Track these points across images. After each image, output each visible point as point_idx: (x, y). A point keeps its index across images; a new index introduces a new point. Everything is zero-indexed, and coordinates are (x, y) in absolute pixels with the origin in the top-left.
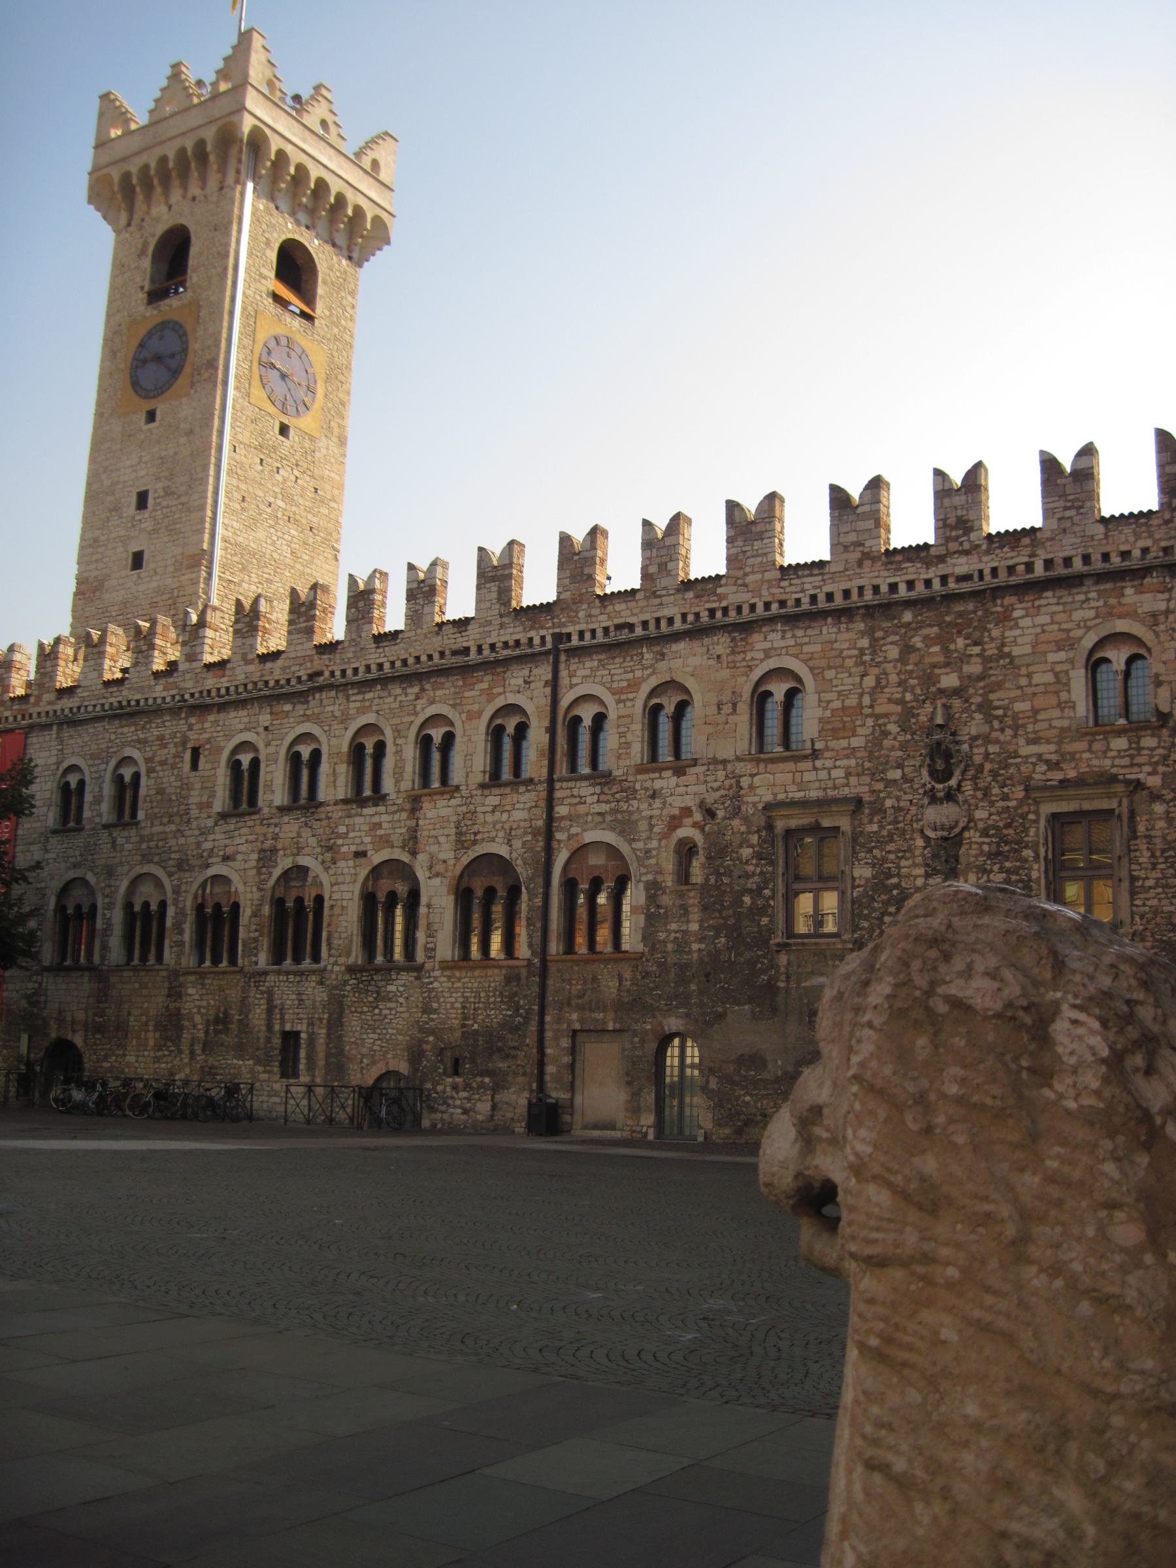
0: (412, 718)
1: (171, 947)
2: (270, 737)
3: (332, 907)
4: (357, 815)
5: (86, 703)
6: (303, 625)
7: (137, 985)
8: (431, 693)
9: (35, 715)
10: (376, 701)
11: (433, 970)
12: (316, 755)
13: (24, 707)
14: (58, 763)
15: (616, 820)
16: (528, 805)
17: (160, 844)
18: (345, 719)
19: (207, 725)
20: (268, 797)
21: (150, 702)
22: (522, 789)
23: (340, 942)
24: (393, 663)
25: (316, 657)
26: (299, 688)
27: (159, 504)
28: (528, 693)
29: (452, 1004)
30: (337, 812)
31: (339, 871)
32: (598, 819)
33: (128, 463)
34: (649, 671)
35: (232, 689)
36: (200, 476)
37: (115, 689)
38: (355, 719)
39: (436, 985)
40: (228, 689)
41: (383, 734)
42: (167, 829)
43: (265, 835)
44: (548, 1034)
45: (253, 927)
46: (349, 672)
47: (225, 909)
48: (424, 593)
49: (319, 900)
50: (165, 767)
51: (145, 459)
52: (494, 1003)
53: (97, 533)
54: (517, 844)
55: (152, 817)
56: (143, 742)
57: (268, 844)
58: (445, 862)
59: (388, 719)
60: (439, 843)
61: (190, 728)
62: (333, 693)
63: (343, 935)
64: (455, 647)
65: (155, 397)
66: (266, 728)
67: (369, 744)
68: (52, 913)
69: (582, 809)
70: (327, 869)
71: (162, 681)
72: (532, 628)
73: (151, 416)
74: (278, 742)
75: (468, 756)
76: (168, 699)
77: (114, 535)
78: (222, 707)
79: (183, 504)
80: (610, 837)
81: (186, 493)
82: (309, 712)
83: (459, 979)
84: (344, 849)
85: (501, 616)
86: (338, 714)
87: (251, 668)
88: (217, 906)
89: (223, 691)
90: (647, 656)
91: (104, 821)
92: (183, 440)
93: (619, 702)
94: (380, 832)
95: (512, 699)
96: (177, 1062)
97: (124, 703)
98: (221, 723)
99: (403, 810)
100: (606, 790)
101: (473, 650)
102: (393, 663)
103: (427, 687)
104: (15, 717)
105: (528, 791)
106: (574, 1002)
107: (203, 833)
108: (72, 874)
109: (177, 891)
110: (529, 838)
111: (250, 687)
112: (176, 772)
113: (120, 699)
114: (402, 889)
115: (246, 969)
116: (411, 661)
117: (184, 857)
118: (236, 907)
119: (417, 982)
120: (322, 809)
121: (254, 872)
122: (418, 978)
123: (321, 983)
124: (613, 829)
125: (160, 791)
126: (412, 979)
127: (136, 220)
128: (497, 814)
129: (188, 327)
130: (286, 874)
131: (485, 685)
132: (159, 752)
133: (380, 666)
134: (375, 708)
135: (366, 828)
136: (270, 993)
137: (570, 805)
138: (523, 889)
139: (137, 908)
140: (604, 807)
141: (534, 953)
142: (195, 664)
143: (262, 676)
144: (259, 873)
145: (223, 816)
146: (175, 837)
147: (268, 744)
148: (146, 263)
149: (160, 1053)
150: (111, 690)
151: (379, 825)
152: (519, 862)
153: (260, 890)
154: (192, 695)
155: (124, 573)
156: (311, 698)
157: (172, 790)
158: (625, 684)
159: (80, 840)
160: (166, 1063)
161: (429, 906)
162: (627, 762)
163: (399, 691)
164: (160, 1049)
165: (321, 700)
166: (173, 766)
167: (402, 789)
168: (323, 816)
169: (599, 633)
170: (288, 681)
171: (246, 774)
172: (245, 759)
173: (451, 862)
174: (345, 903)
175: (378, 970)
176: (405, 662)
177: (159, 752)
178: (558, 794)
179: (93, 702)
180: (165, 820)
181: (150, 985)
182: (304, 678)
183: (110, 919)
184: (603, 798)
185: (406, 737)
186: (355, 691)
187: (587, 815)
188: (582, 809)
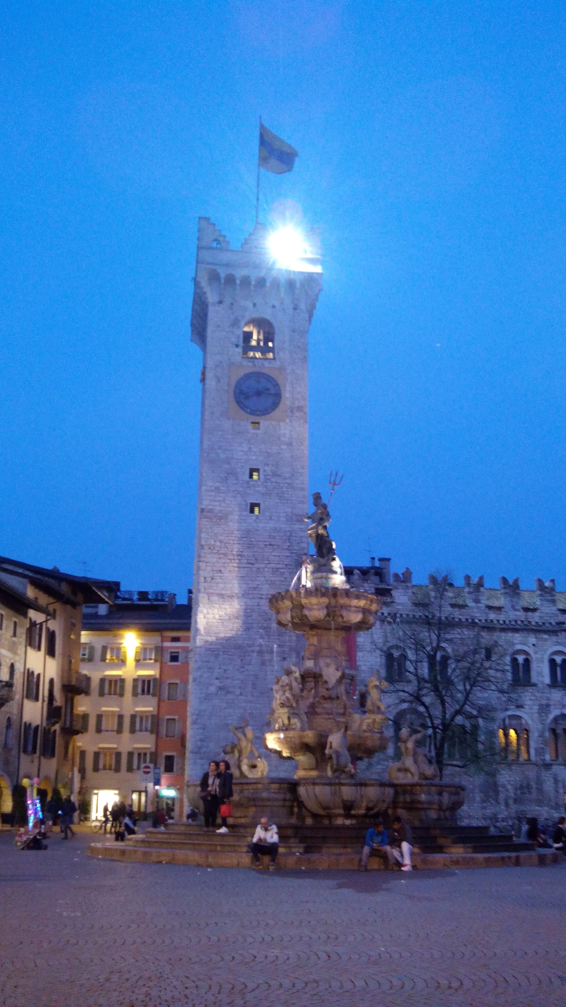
26: (550, 628)
35: (507, 622)
40: (504, 621)
53: (218, 484)
57: (544, 702)
65: (258, 415)
79: (289, 484)
81: (290, 478)
87: (518, 613)
89: (501, 622)
92: (284, 447)
96: (498, 809)
127: (227, 301)
129: (280, 382)
142: (479, 605)
143: (527, 618)
144: (540, 716)
147: (536, 653)
149: (484, 805)
155: (245, 513)
156: (559, 634)
160: (491, 810)
164: (484, 801)
172: (521, 659)
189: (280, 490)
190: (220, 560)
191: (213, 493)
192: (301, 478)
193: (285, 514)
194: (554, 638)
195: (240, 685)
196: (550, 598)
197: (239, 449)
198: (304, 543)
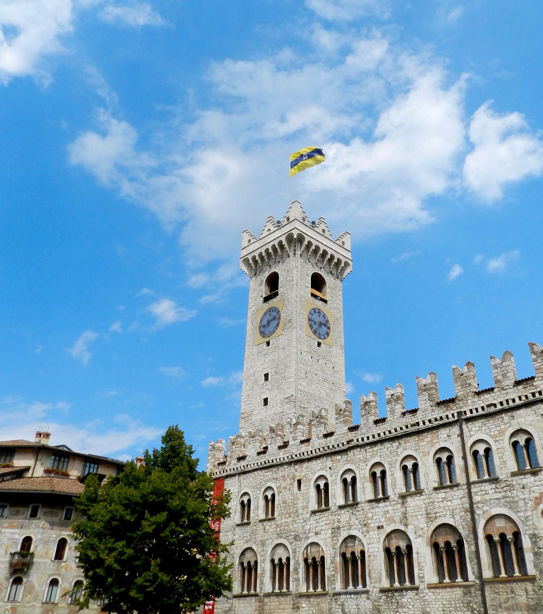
0: (397, 458)
1: (293, 582)
2: (332, 472)
3: (369, 556)
4: (376, 507)
5: (250, 463)
6: (343, 419)
7: (278, 603)
9: (228, 470)
10: (379, 451)
14: (239, 492)
16: (460, 497)
17: (286, 528)
18: (366, 461)
19: (303, 469)
20: (334, 501)
21: (278, 460)
22: (455, 489)
23: (375, 575)
24: (384, 433)
27: (273, 378)
28: (450, 441)
29: (437, 608)
30: (367, 506)
31: (371, 537)
33: (260, 363)
37: (263, 455)
38: (370, 460)
39: (427, 597)
40: (311, 451)
42: (288, 520)
43: (334, 520)
45: (332, 569)
46: (365, 439)
47: (317, 560)
48: (394, 400)
49: (363, 553)
50: (286, 490)
52: (460, 607)
54: (457, 517)
55: (281, 515)
56: (276, 479)
58: (422, 529)
59: (385, 459)
60: (418, 519)
61: (296, 471)
62: (359, 449)
63: (376, 571)
64: (413, 423)
66: (330, 468)
67: (378, 471)
68: (237, 566)
69: (487, 497)
70: (365, 536)
71: (283, 450)
74: (336, 474)
76: (286, 458)
78: (309, 460)
82: (349, 459)
84: (372, 525)
85: (432, 406)
86: (362, 459)
88: (314, 559)
89: (309, 453)
91: (260, 519)
94: (388, 516)
95: (443, 445)
97: (267, 462)
98: (310, 467)
99: (398, 503)
101: (421, 424)
102: (384, 433)
103: (402, 442)
105: (458, 490)
107: (305, 521)
108: (246, 546)
109: (294, 552)
110: (463, 514)
111: (321, 449)
112: (291, 492)
113: (265, 460)
114: (403, 545)
115: (330, 592)
116: (393, 431)
117: (297, 534)
118: (323, 558)
119: (416, 597)
120: (359, 506)
121: (330, 539)
122: (417, 594)
123: (368, 598)
125: (284, 502)
126: (415, 594)
130: (345, 540)
131: (429, 439)
132: (283, 483)
134: (378, 455)
135: (381, 514)
136: (343, 605)
137: (481, 495)
138: (465, 542)
139: (276, 562)
142: (296, 441)
143: (326, 444)
145: (314, 512)
146: (292, 524)
150: (261, 456)
151: (388, 512)
153: (333, 548)
155: (260, 408)
157: (290, 501)
159: (249, 528)
161: (417, 553)
165: (354, 453)
166: (290, 490)
167: (396, 493)
168: (360, 509)
170: (338, 445)
171: (323, 491)
172: (322, 483)
173: (425, 529)
174: (375, 554)
175: (396, 590)
176: (390, 432)
177: (283, 483)
179: (253, 462)
180: (287, 516)
181: (284, 602)
182: (345, 443)
183: (264, 568)
185: (395, 467)
186: (369, 447)
187: (490, 500)
188: (487, 497)
191: (246, 400)
194: (345, 457)
196: (343, 419)
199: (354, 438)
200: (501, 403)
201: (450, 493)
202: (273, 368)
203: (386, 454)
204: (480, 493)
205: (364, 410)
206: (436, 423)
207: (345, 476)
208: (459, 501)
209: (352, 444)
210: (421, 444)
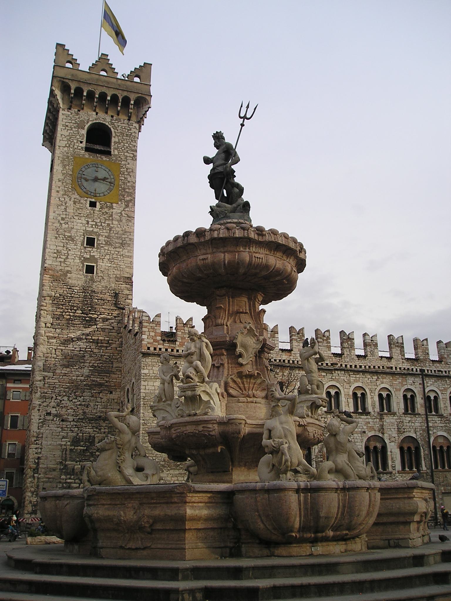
0: (376, 387)
4: (359, 418)
8: (382, 380)
10: (361, 378)
11: (396, 474)
12: (337, 394)
13: (172, 345)
15: (446, 429)
18: (349, 383)
22: (417, 416)
25: (333, 357)
26: (327, 368)
31: (355, 438)
32: (441, 428)
34: (449, 386)
36: (128, 243)
39: (397, 479)
40: (293, 361)
41: (364, 390)
44: (436, 494)
46: (348, 366)
48: (374, 345)
51: (90, 223)
53: (59, 248)
54: (418, 434)
58: (394, 437)
62: (343, 372)
64: (388, 366)
72: (413, 365)
73: (93, 205)
75: (398, 403)
77: (73, 253)
79: (118, 252)
80: (445, 434)
82: (333, 377)
83: (405, 477)
89: (291, 362)
90: (448, 381)
93: (442, 394)
99: (377, 418)
100: (442, 419)
101: (394, 369)
102: (365, 366)
104: (166, 350)
106: (441, 484)
110: (422, 432)
114: (379, 445)
116: (372, 367)
119: (390, 478)
122: (390, 477)
124: (445, 432)
128: (410, 423)
131: (400, 381)
133: (361, 367)
134: (361, 381)
140: (442, 425)
141: (427, 469)
148: (84, 132)
152: (419, 439)
154: (275, 360)
156: (333, 372)
158: (443, 389)
161: (391, 452)
162: (447, 412)
163: (369, 377)
167: (375, 411)
169: (433, 372)
173: (397, 438)
178: (429, 419)
182: (329, 364)
184: (442, 422)
186: (352, 373)
189: (111, 256)
190: (58, 310)
191: (56, 255)
192: (129, 248)
193: (115, 276)
194: (329, 376)
195: (73, 413)
197: (80, 221)
198: (129, 299)
199: (338, 363)
200: (446, 372)
201: (414, 418)
202: (102, 236)
203: (367, 383)
204: (432, 422)
205: (346, 344)
206: (405, 372)
207: (328, 390)
208: (419, 424)
209: (337, 367)
210: (394, 382)
